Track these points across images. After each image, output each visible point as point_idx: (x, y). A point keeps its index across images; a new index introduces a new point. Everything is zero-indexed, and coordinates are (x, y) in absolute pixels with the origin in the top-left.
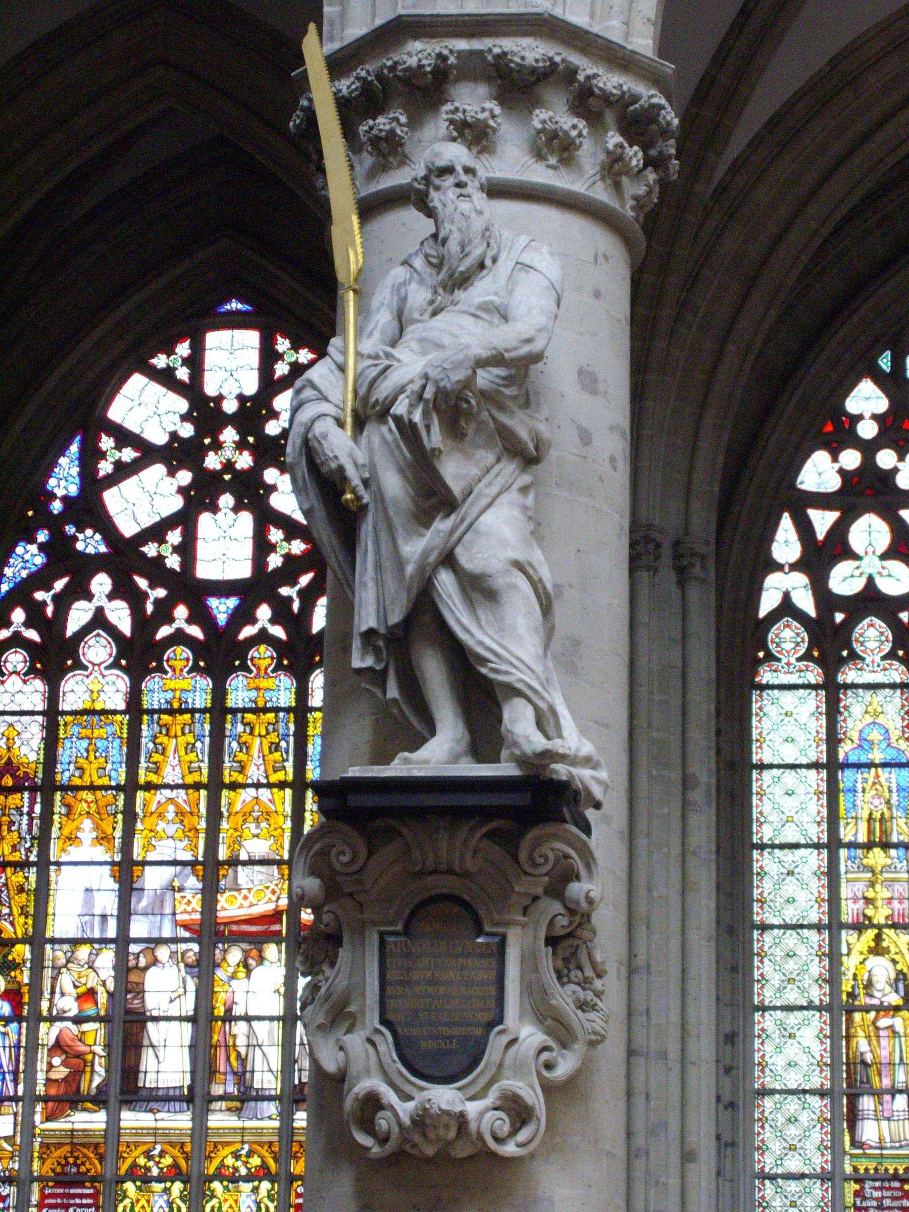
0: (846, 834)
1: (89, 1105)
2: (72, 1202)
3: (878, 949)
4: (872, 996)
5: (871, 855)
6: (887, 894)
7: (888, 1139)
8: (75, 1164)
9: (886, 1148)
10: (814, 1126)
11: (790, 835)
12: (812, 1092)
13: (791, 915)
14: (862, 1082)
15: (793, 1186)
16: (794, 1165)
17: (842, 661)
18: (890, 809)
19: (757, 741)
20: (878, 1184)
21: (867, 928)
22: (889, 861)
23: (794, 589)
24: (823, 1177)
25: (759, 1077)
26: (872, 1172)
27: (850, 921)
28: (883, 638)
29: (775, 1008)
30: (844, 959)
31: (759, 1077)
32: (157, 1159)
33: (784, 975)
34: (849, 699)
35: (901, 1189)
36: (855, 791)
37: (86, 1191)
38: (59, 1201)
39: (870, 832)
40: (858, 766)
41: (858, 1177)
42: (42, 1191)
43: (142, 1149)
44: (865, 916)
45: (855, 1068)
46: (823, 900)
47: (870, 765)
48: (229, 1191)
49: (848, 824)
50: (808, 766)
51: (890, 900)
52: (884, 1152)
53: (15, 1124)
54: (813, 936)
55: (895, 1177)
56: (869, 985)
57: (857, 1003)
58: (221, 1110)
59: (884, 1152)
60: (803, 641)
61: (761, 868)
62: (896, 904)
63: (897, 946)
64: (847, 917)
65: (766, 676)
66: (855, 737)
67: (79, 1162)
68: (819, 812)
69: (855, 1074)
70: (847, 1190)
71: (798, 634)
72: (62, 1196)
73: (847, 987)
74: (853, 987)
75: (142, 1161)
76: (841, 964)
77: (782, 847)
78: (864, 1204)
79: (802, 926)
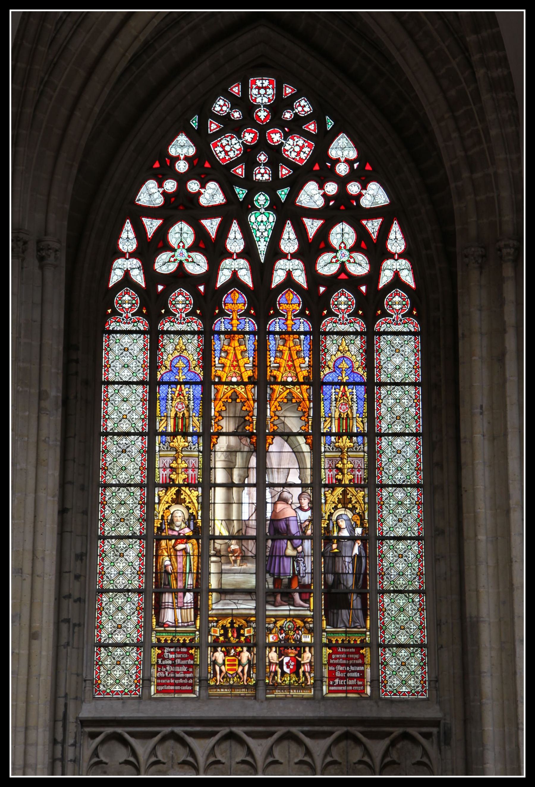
0: (160, 427)
3: (178, 500)
4: (174, 530)
5: (175, 440)
6: (184, 465)
7: (180, 621)
9: (179, 627)
10: (134, 613)
11: (125, 427)
12: (133, 591)
13: (123, 477)
14: (165, 584)
15: (119, 651)
16: (119, 638)
17: (161, 317)
18: (188, 411)
19: (105, 366)
20: (172, 650)
21: (171, 486)
22: (187, 444)
23: (132, 269)
24: (138, 645)
25: (100, 582)
26: (169, 642)
27: (161, 482)
28: (188, 302)
29: (112, 537)
30: (156, 506)
31: (100, 582)
33: (118, 516)
34: (165, 340)
35: (187, 652)
36: (167, 400)
39: (175, 425)
40: (169, 383)
41: (161, 645)
44: (170, 478)
45: (161, 575)
46: (144, 469)
47: (177, 383)
49: (161, 420)
50: (137, 383)
51: (187, 469)
52: (177, 629)
54: (138, 492)
55: (184, 645)
56: (172, 522)
57: (163, 534)
59: (177, 629)
60: (137, 303)
61: (105, 447)
62: (190, 472)
63: (190, 498)
64: (159, 480)
65: (113, 326)
66: (168, 364)
68: (143, 413)
69: (161, 579)
70: (153, 654)
71: (134, 298)
73: (157, 524)
74: (161, 524)
76: (154, 509)
77: (119, 434)
78: (164, 663)
79: (130, 485)
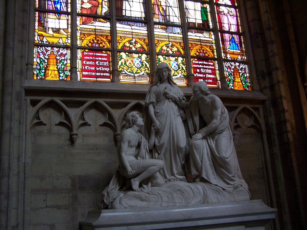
1: (102, 20)
2: (97, 59)
8: (97, 43)
32: (134, 44)
37: (103, 55)
38: (91, 58)
42: (83, 53)
43: (127, 40)
48: (166, 59)
53: (68, 24)
58: (158, 28)
67: (99, 42)
72: (92, 56)
75: (127, 44)
